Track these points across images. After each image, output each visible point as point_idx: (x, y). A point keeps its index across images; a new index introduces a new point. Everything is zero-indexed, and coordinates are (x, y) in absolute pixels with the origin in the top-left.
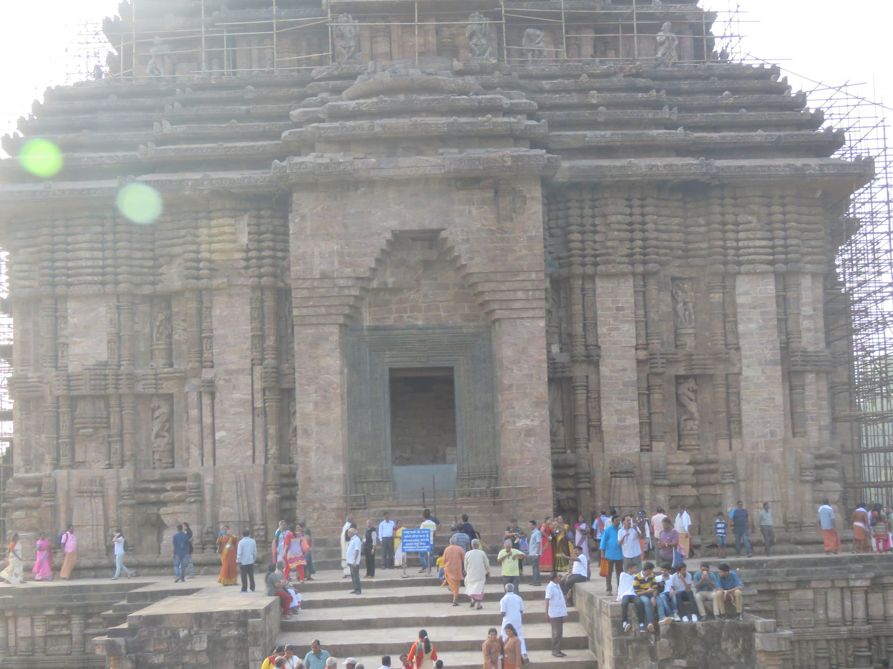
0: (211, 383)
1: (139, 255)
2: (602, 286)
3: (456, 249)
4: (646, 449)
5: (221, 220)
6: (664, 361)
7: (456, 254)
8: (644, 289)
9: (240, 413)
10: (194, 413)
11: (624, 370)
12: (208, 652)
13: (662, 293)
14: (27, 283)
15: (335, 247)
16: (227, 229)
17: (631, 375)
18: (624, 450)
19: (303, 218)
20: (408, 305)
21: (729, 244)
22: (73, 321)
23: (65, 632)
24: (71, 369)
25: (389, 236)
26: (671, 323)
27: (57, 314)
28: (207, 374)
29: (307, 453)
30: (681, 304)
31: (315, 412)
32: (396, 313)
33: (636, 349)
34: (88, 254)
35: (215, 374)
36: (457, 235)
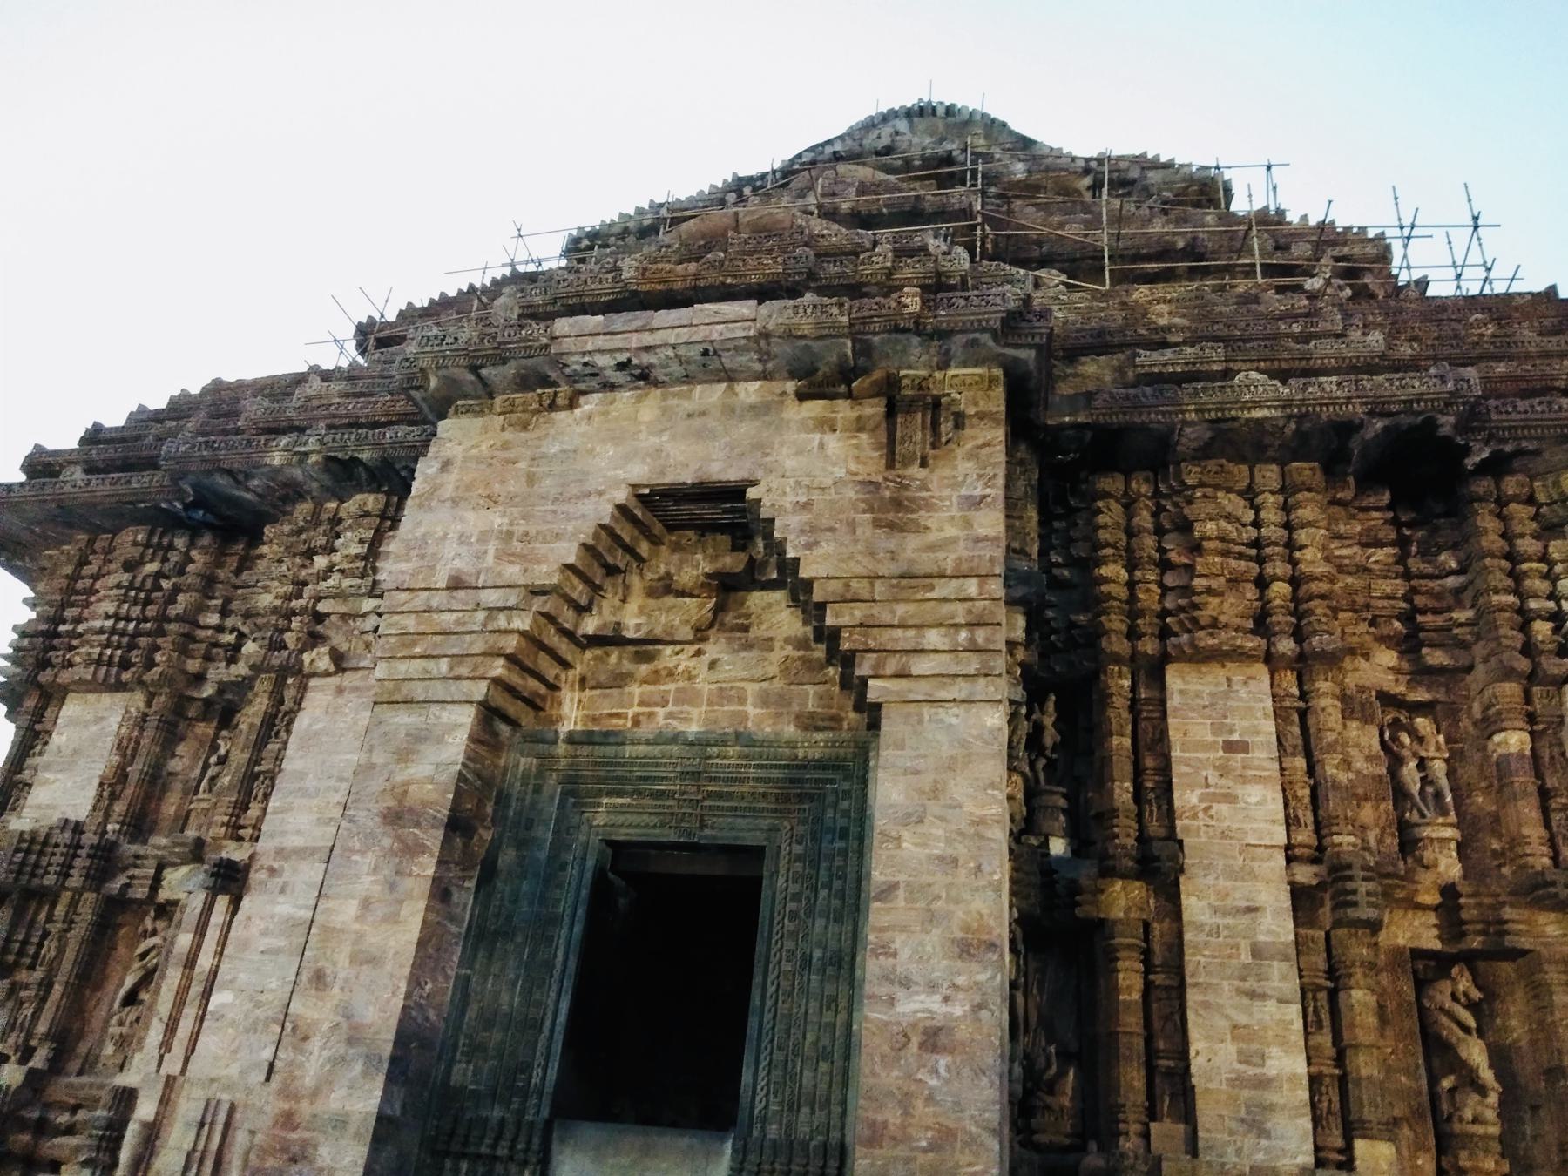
3: (777, 523)
6: (1371, 886)
8: (1301, 704)
9: (277, 951)
11: (1251, 910)
13: (1354, 724)
15: (497, 520)
17: (1278, 926)
18: (1260, 1157)
19: (446, 465)
20: (672, 687)
25: (622, 496)
26: (1389, 805)
27: (38, 727)
29: (305, 1039)
31: (357, 926)
32: (641, 704)
34: (110, 608)
35: (252, 857)
36: (785, 493)
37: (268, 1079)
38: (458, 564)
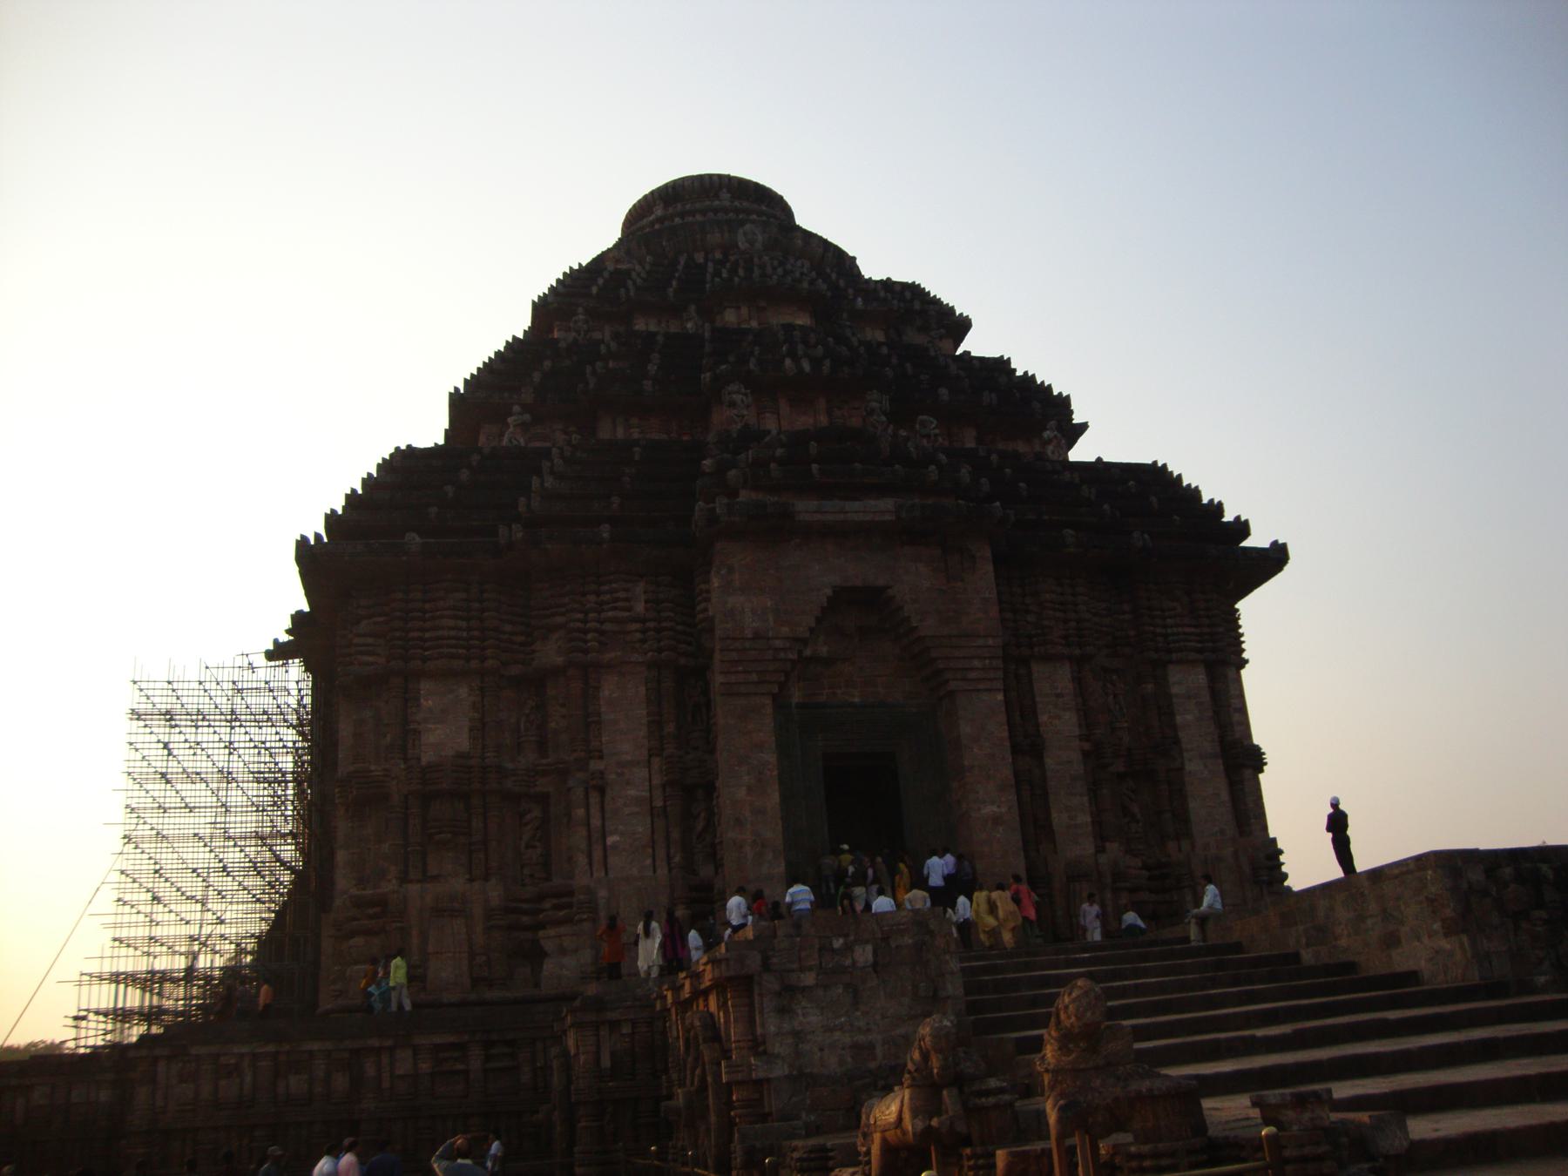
0: (602, 773)
1: (508, 628)
2: (1038, 670)
4: (1100, 850)
5: (614, 585)
7: (906, 614)
10: (581, 812)
12: (875, 965)
14: (371, 659)
16: (622, 595)
21: (1159, 630)
22: (427, 703)
23: (460, 1067)
24: (424, 761)
25: (829, 592)
28: (595, 765)
30: (1112, 697)
33: (1081, 740)
34: (451, 623)
37: (655, 871)
38: (754, 624)
